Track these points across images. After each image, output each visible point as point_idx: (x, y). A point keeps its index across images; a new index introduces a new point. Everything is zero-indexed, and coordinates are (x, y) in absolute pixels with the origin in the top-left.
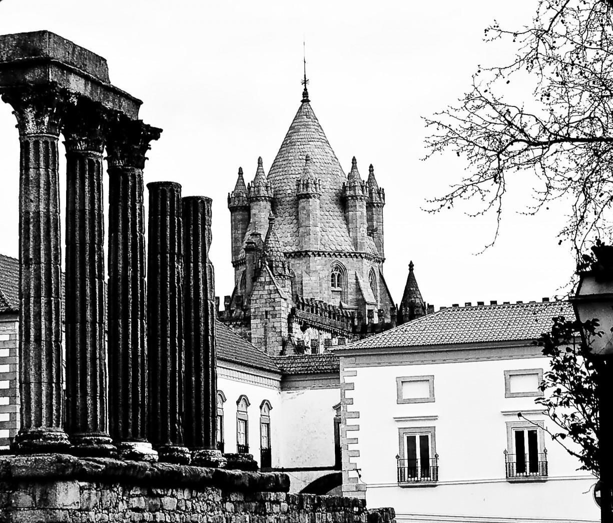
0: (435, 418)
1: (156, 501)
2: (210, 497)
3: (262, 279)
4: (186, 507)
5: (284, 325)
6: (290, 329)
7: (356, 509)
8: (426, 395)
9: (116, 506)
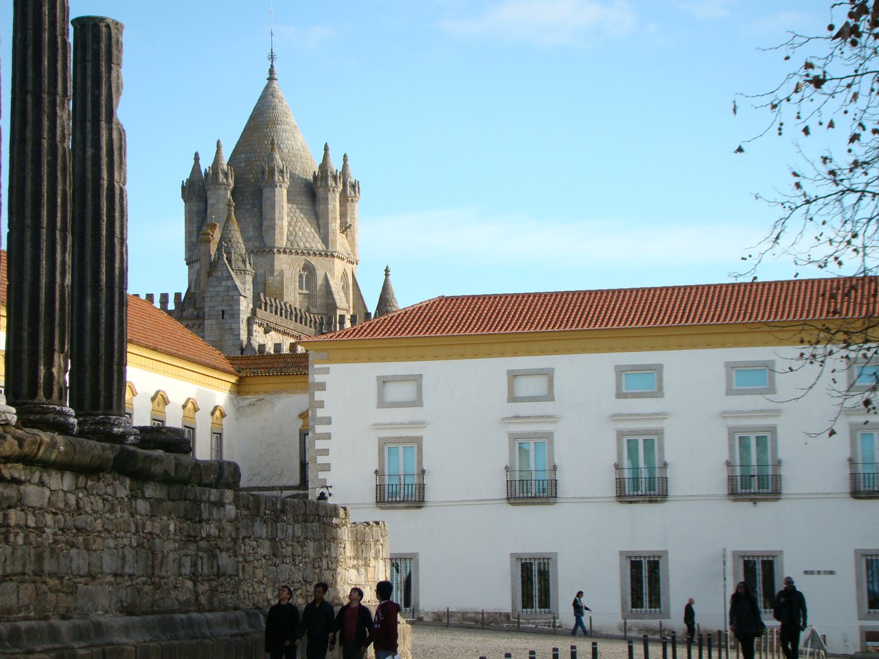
0: (422, 424)
2: (109, 490)
3: (219, 274)
4: (66, 504)
5: (243, 327)
6: (250, 333)
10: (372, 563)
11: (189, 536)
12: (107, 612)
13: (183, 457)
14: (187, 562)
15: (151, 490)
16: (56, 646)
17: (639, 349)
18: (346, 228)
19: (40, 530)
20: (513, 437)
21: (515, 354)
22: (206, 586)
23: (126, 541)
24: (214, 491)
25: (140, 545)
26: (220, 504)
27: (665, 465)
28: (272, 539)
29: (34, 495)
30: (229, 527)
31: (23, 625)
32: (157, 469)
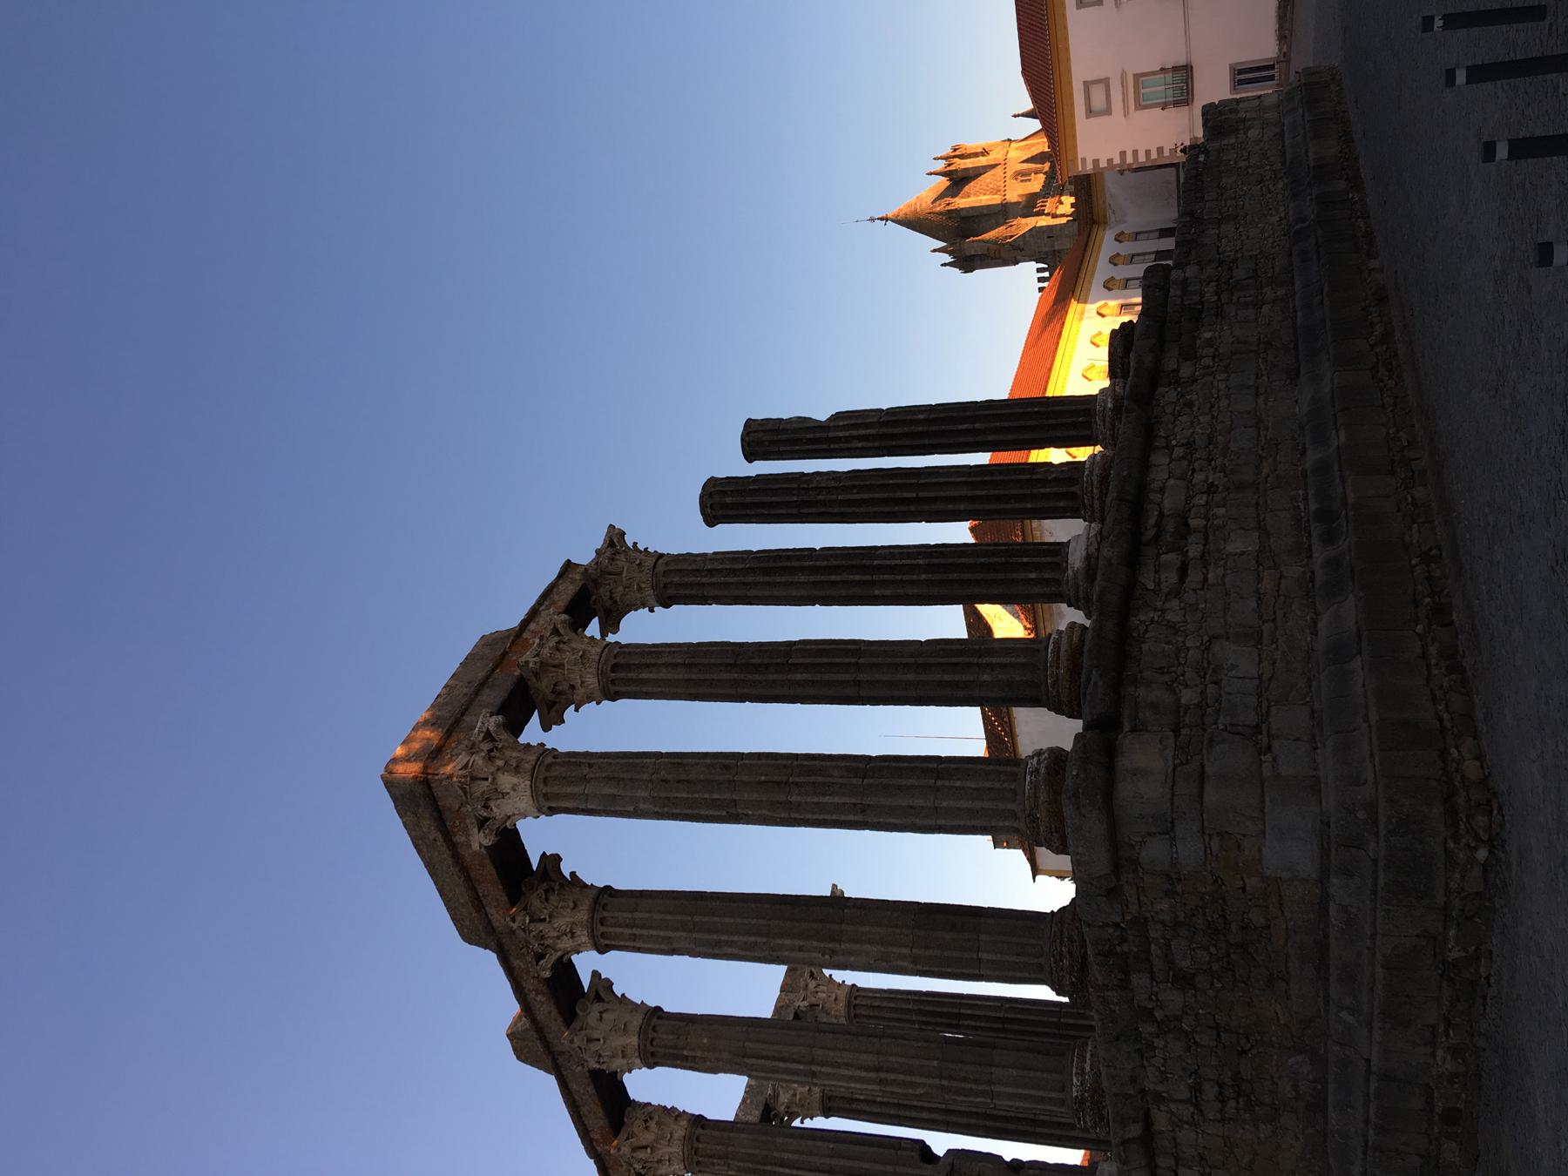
0: (1123, 75)
1: (1170, 526)
2: (1169, 410)
4: (1184, 457)
7: (1201, 158)
8: (1101, 87)
9: (1173, 628)
10: (1242, 115)
11: (1217, 315)
15: (1171, 364)
16: (1336, 468)
18: (985, 153)
19: (1211, 489)
23: (1222, 386)
26: (1185, 283)
29: (1171, 501)
31: (1313, 506)
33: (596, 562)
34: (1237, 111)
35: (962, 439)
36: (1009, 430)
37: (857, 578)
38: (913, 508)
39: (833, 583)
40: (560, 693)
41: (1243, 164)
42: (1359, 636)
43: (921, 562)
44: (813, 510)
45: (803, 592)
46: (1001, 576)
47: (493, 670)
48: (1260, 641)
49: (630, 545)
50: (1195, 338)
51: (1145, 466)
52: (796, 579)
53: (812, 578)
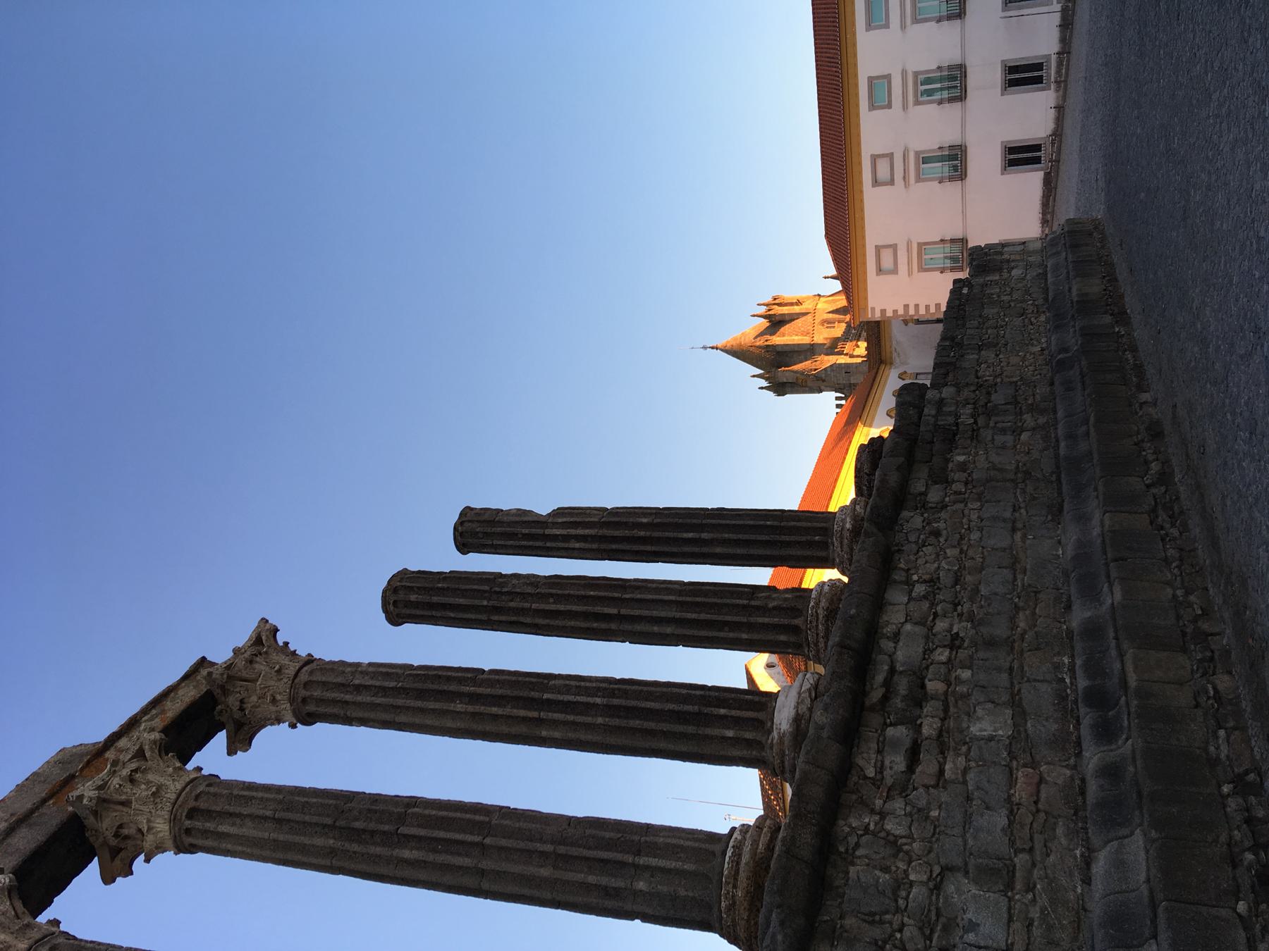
0: (909, 243)
1: (902, 685)
2: (912, 538)
4: (925, 597)
7: (965, 291)
8: (890, 251)
9: (893, 843)
10: (1006, 256)
11: (972, 439)
12: (1059, 542)
13: (886, 449)
14: (1000, 439)
15: (919, 486)
17: (857, 95)
18: (799, 303)
19: (954, 642)
20: (919, 179)
21: (861, 183)
22: (1027, 417)
23: (974, 516)
24: (926, 411)
25: (979, 497)
26: (941, 403)
27: (939, 68)
28: (980, 348)
29: (906, 653)
30: (966, 393)
31: (1082, 683)
32: (894, 478)
33: (229, 666)
34: (1002, 254)
35: (686, 549)
36: (737, 543)
37: (522, 713)
38: (613, 626)
39: (495, 717)
40: (127, 837)
41: (1006, 298)
42: (1154, 906)
43: (598, 700)
44: (503, 618)
45: (459, 724)
46: (691, 729)
47: (44, 801)
48: (1010, 886)
49: (281, 643)
50: (947, 461)
51: (879, 604)
52: (452, 707)
53: (470, 708)
